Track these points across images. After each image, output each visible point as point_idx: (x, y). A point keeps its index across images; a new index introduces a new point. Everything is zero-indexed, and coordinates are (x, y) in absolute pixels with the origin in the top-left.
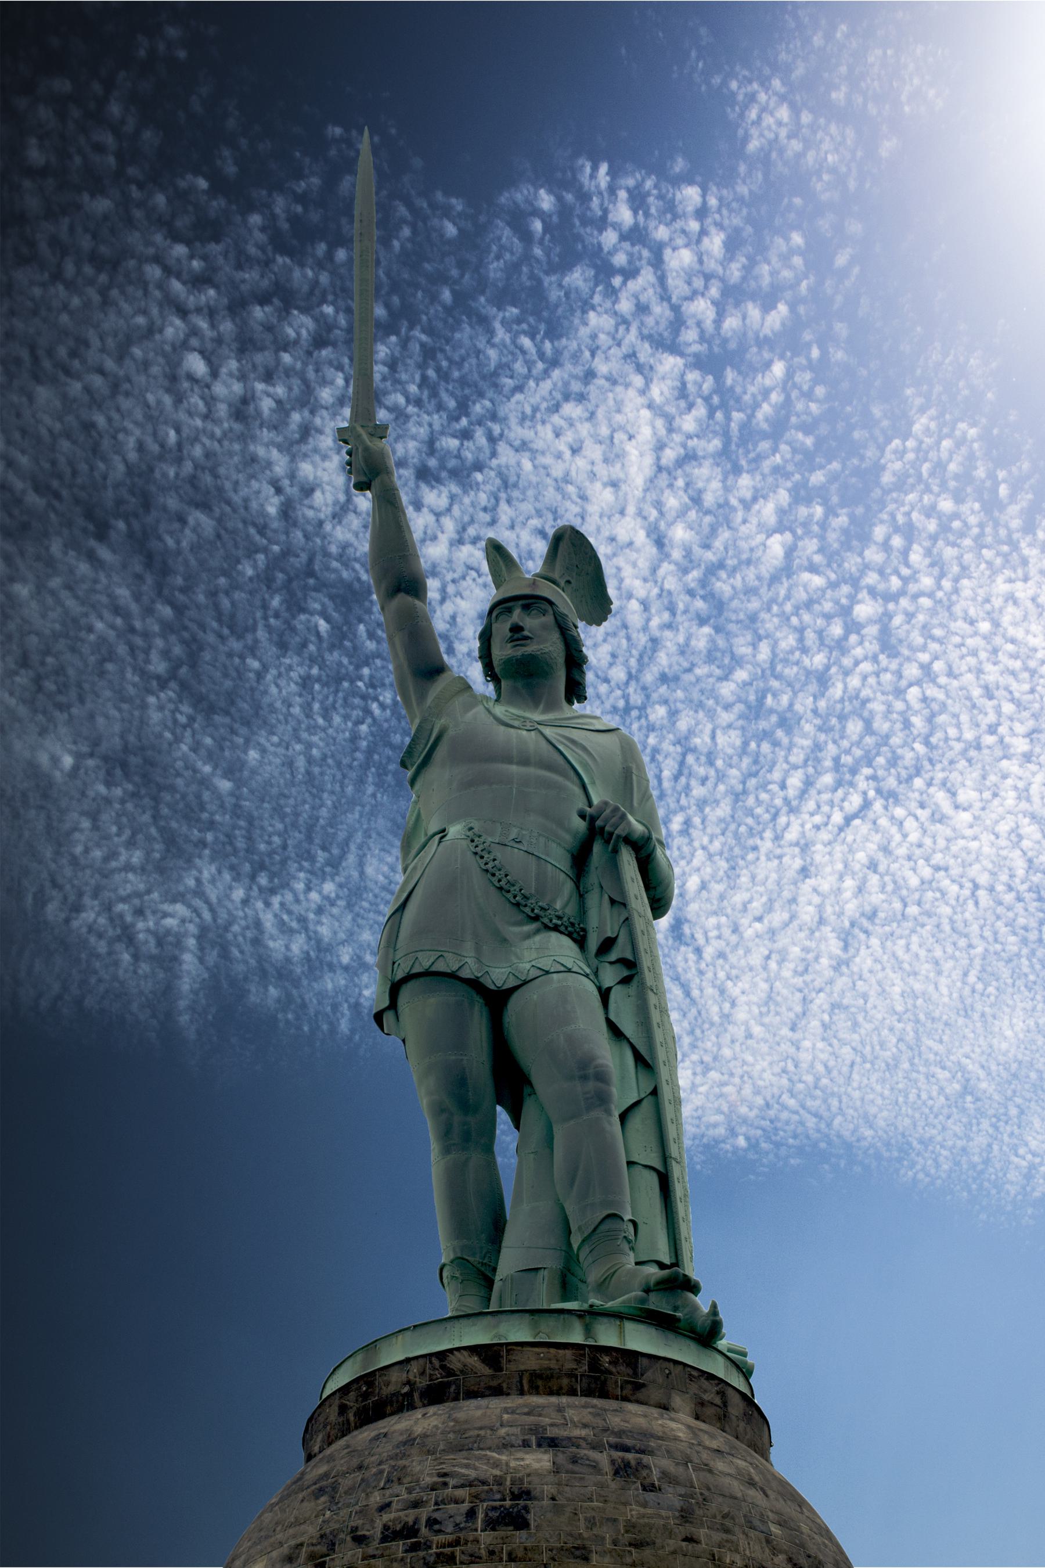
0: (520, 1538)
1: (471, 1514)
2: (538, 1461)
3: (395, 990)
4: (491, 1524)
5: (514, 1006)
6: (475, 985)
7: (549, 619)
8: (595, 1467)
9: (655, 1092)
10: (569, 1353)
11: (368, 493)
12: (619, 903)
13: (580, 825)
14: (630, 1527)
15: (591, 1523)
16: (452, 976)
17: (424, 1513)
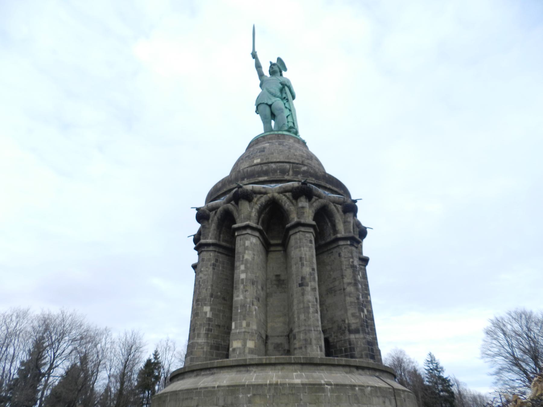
0: (263, 153)
1: (257, 152)
2: (268, 145)
3: (257, 107)
4: (259, 152)
5: (272, 106)
6: (267, 104)
7: (276, 66)
8: (275, 144)
9: (292, 114)
10: (274, 135)
11: (254, 60)
12: (286, 93)
13: (280, 86)
14: (280, 150)
15: (274, 150)
16: (263, 103)
17: (250, 154)
